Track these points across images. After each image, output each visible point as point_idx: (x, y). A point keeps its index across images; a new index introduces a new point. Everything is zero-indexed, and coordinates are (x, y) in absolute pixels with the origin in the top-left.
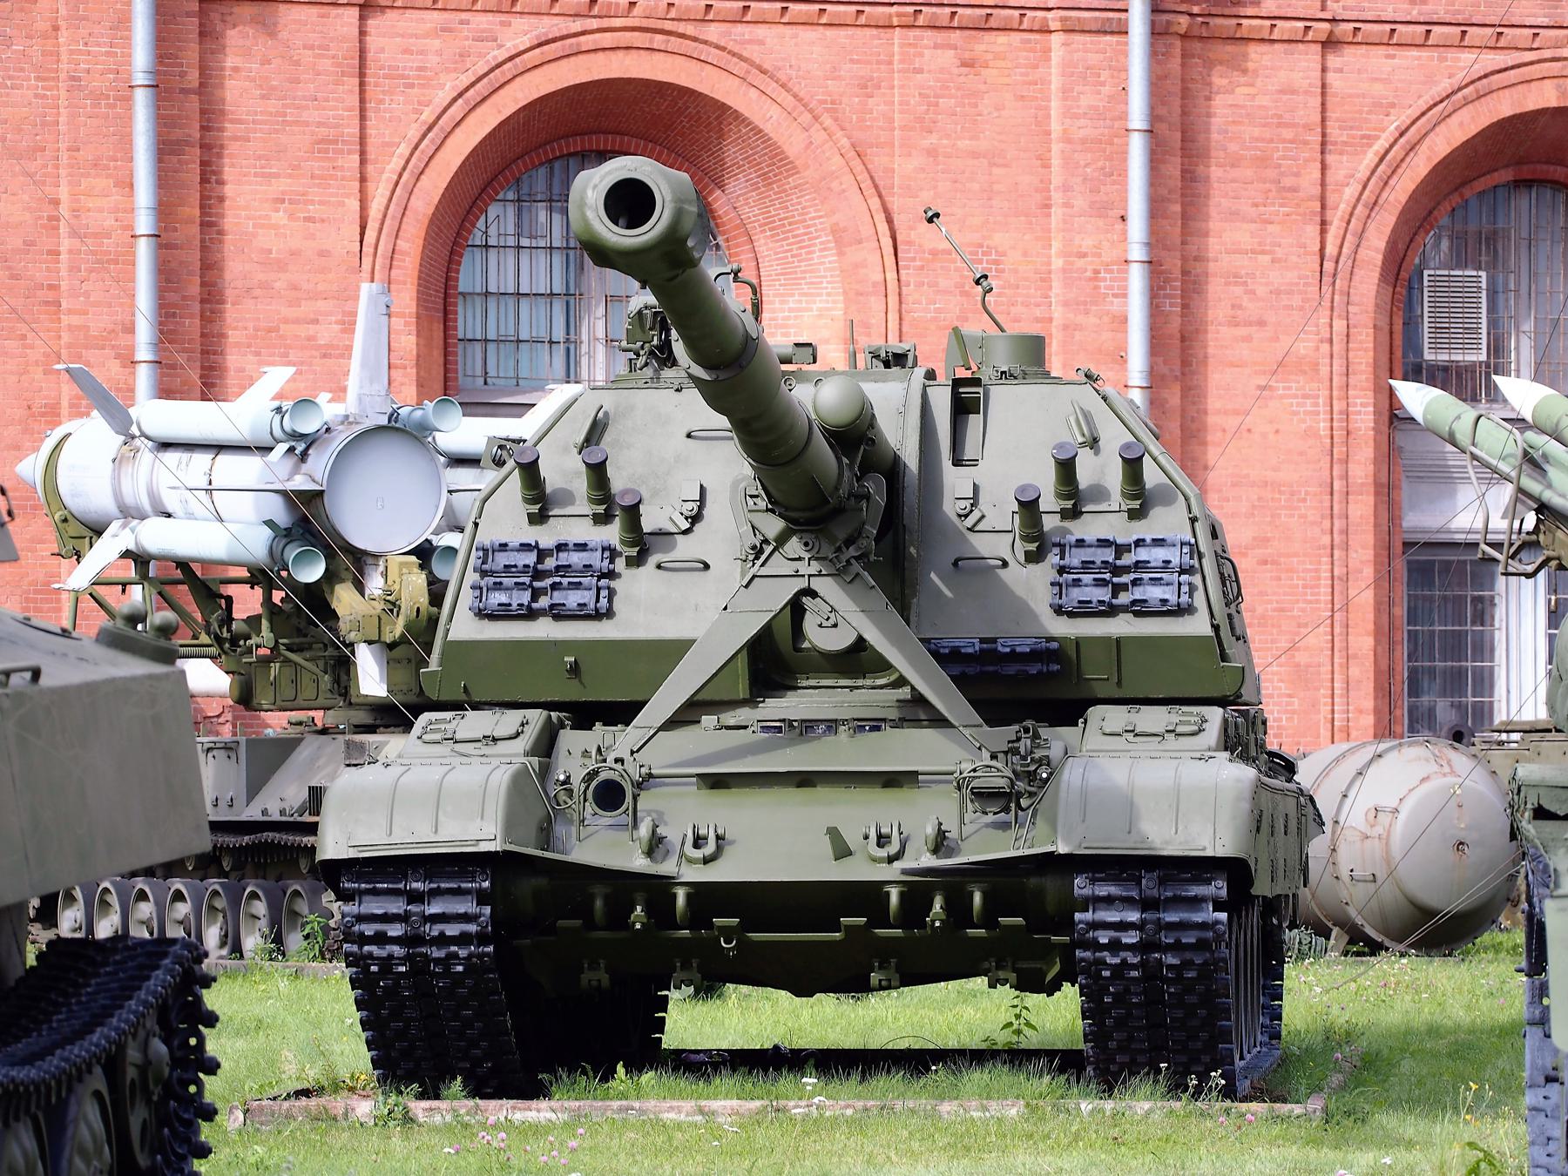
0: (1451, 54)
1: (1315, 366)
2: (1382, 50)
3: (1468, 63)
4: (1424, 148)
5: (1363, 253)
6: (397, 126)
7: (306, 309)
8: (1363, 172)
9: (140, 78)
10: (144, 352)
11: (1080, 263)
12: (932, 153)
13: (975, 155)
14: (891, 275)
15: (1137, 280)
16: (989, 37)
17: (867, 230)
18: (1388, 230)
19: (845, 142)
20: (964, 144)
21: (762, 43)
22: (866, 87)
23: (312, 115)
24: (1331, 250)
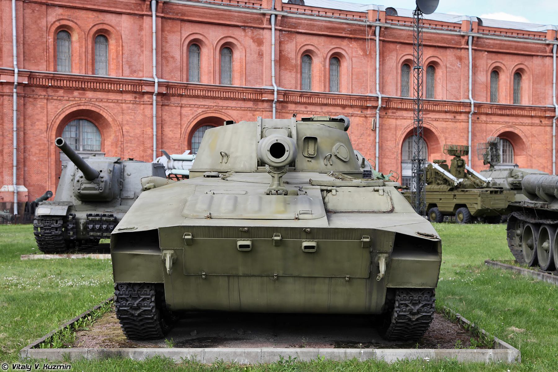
6: (185, 121)
7: (174, 144)
9: (154, 115)
10: (155, 149)
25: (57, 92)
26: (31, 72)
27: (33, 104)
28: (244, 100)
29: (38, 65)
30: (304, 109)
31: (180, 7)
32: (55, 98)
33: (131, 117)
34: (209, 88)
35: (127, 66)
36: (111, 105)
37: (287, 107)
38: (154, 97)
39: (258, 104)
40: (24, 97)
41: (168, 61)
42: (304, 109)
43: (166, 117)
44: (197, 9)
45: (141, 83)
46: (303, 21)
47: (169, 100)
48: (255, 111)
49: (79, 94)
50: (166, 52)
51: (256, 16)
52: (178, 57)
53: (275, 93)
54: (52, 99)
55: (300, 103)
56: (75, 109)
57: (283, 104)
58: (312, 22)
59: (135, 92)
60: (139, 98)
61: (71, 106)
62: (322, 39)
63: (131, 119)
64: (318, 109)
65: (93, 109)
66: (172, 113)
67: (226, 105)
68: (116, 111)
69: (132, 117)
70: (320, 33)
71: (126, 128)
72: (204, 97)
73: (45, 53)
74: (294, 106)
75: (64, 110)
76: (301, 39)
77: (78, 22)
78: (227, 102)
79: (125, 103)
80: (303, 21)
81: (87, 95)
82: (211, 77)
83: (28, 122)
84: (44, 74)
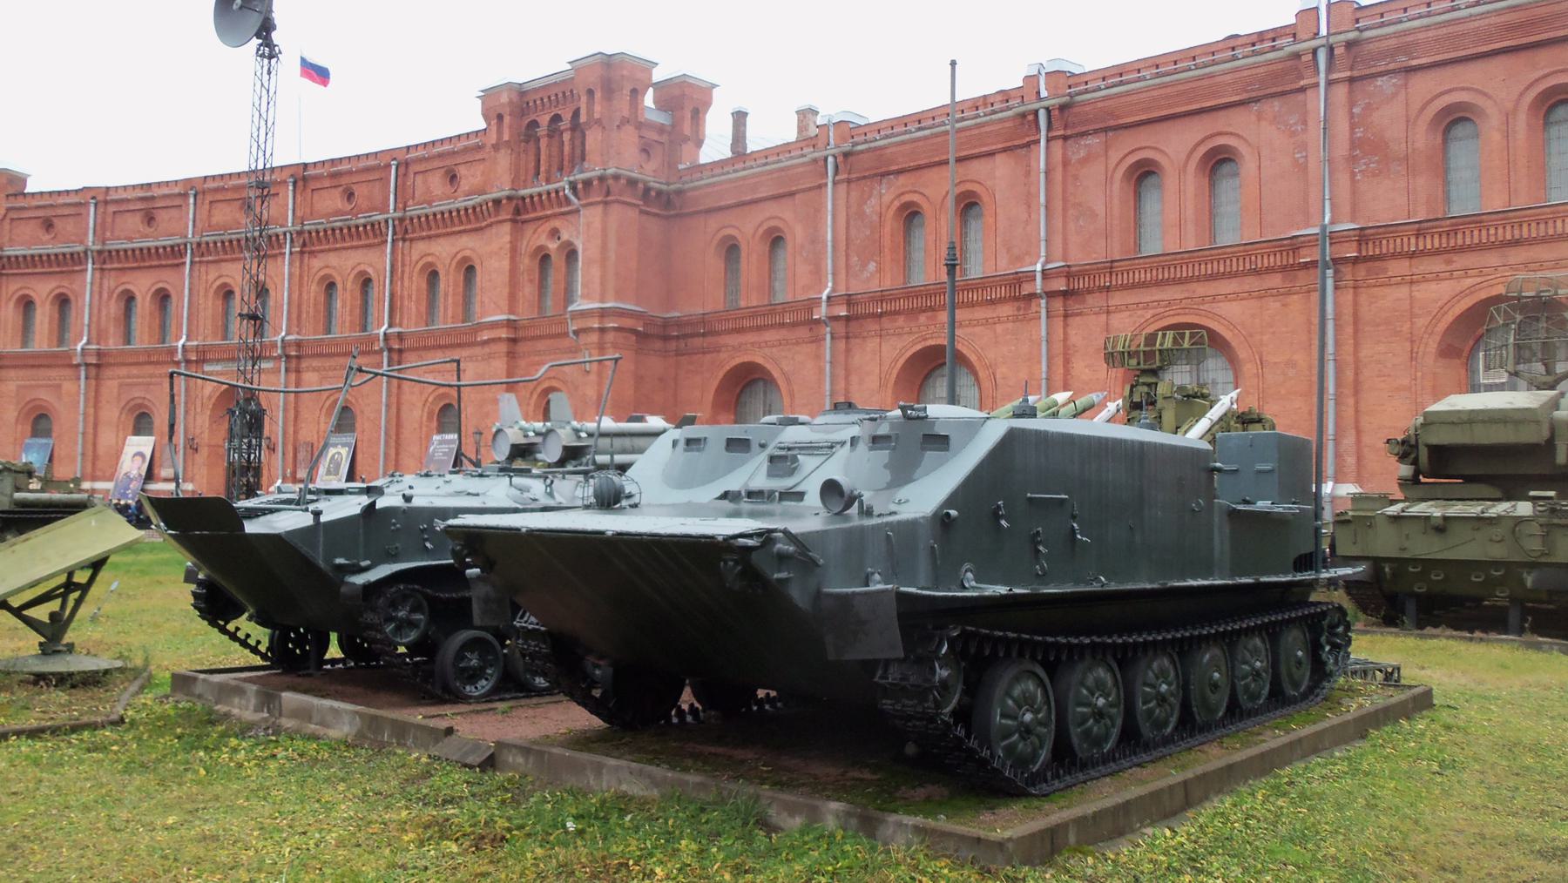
3: (1469, 282)
28: (1256, 272)
30: (1443, 267)
31: (1100, 105)
34: (1165, 260)
36: (978, 329)
37: (1386, 270)
38: (1043, 302)
40: (847, 338)
42: (1443, 267)
43: (1076, 337)
44: (1135, 97)
45: (1020, 279)
46: (1421, 36)
47: (1084, 302)
51: (1280, 66)
52: (1100, 209)
55: (1423, 253)
56: (919, 347)
57: (1370, 264)
58: (1450, 29)
59: (1016, 299)
61: (914, 343)
62: (1497, 66)
64: (1492, 259)
70: (1485, 49)
71: (1001, 371)
72: (1159, 283)
74: (1406, 263)
76: (1423, 86)
77: (926, 192)
78: (1215, 284)
79: (1000, 322)
80: (1421, 36)
83: (854, 379)
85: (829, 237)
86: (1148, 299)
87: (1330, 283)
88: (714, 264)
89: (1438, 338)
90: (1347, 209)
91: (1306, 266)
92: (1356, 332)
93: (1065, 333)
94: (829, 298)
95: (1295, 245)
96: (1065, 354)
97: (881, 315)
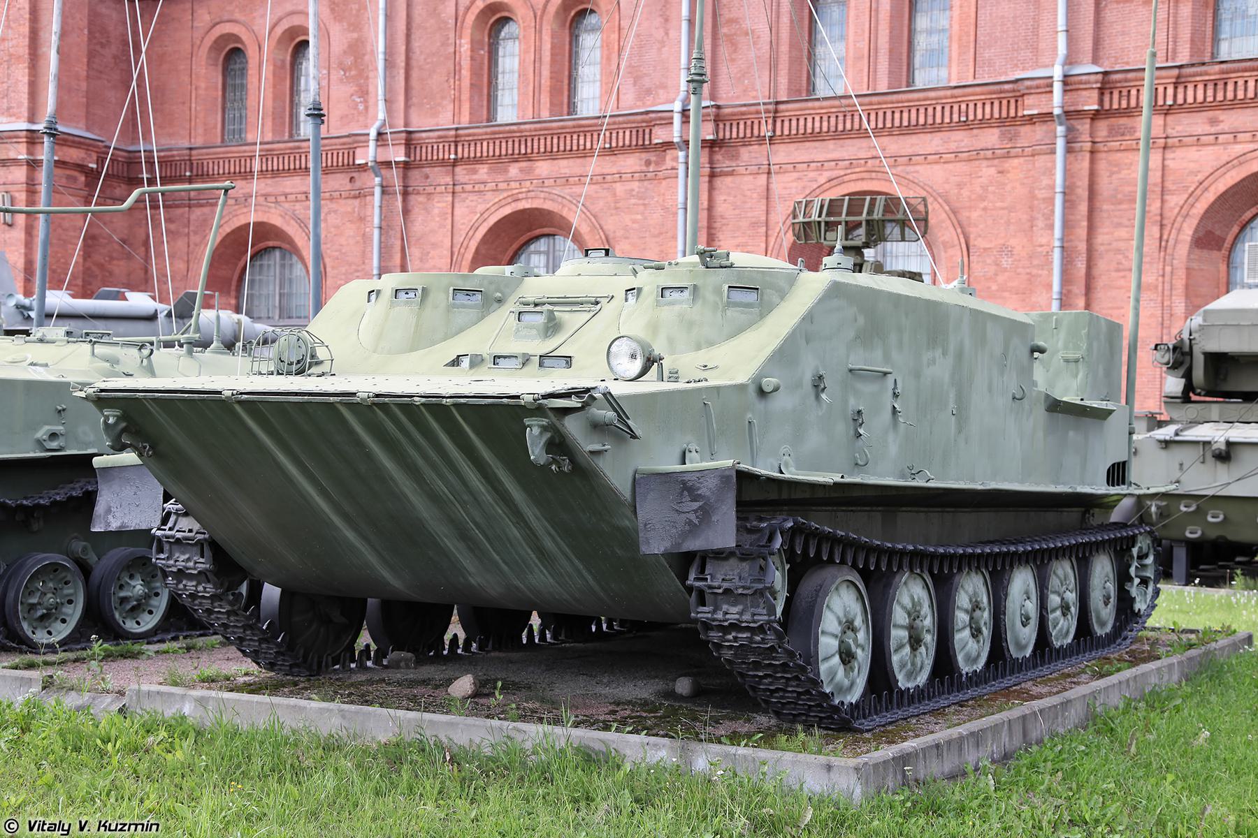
0: (1229, 147)
1: (1156, 287)
2: (1195, 148)
3: (1238, 149)
4: (1212, 189)
5: (1181, 237)
8: (1181, 203)
11: (1040, 249)
12: (985, 209)
13: (1003, 209)
14: (966, 259)
15: (1057, 254)
16: (1010, 160)
17: (956, 242)
18: (1194, 226)
19: (947, 208)
20: (999, 204)
21: (917, 172)
22: (960, 186)
23: (749, 215)
24: (1165, 237)
25: (475, 172)
26: (410, 132)
27: (426, 209)
28: (966, 125)
29: (435, 114)
32: (469, 187)
33: (634, 217)
35: (631, 81)
39: (1017, 135)
41: (734, 45)
47: (736, 157)
48: (1008, 156)
49: (521, 170)
50: (731, 21)
53: (1057, 88)
54: (464, 192)
56: (507, 211)
59: (644, 148)
60: (657, 164)
63: (634, 221)
65: (548, 206)
66: (739, 193)
67: (909, 151)
68: (601, 203)
69: (639, 217)
73: (452, 81)
75: (485, 215)
78: (913, 139)
81: (537, 172)
82: (862, 70)
84: (437, 134)
85: (381, 48)
86: (820, 157)
87: (1060, 144)
88: (207, 77)
89: (1195, 222)
90: (1087, 45)
91: (1031, 120)
92: (1091, 210)
93: (711, 199)
94: (379, 134)
95: (1016, 91)
96: (710, 227)
97: (455, 163)
